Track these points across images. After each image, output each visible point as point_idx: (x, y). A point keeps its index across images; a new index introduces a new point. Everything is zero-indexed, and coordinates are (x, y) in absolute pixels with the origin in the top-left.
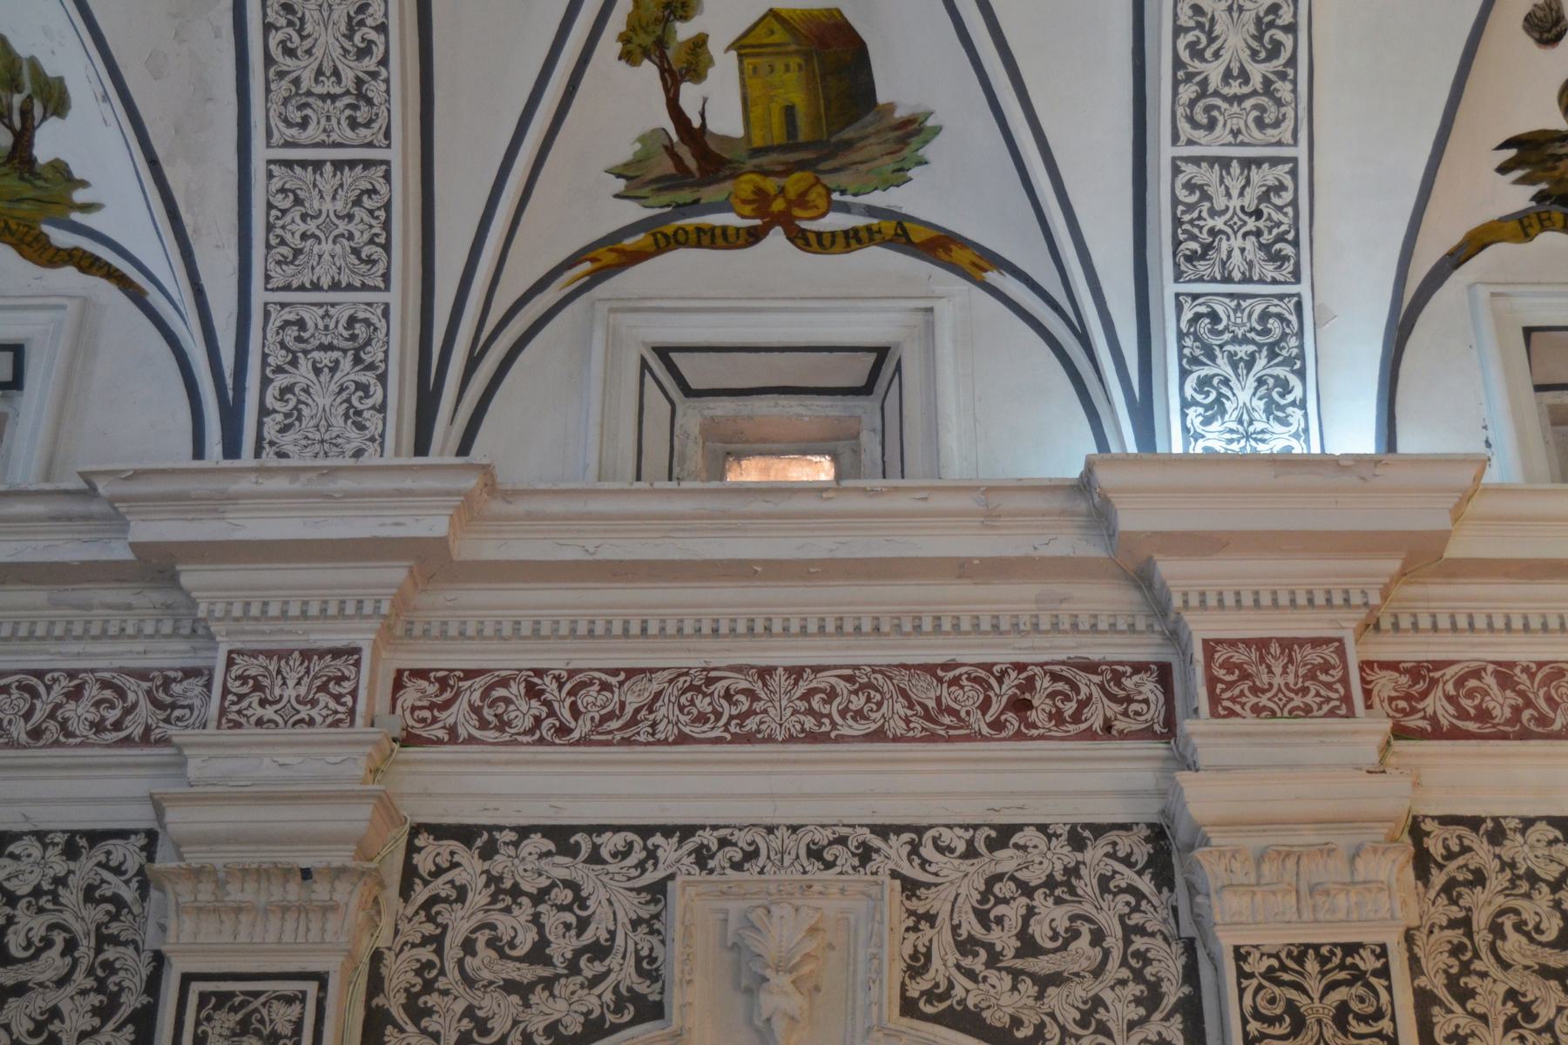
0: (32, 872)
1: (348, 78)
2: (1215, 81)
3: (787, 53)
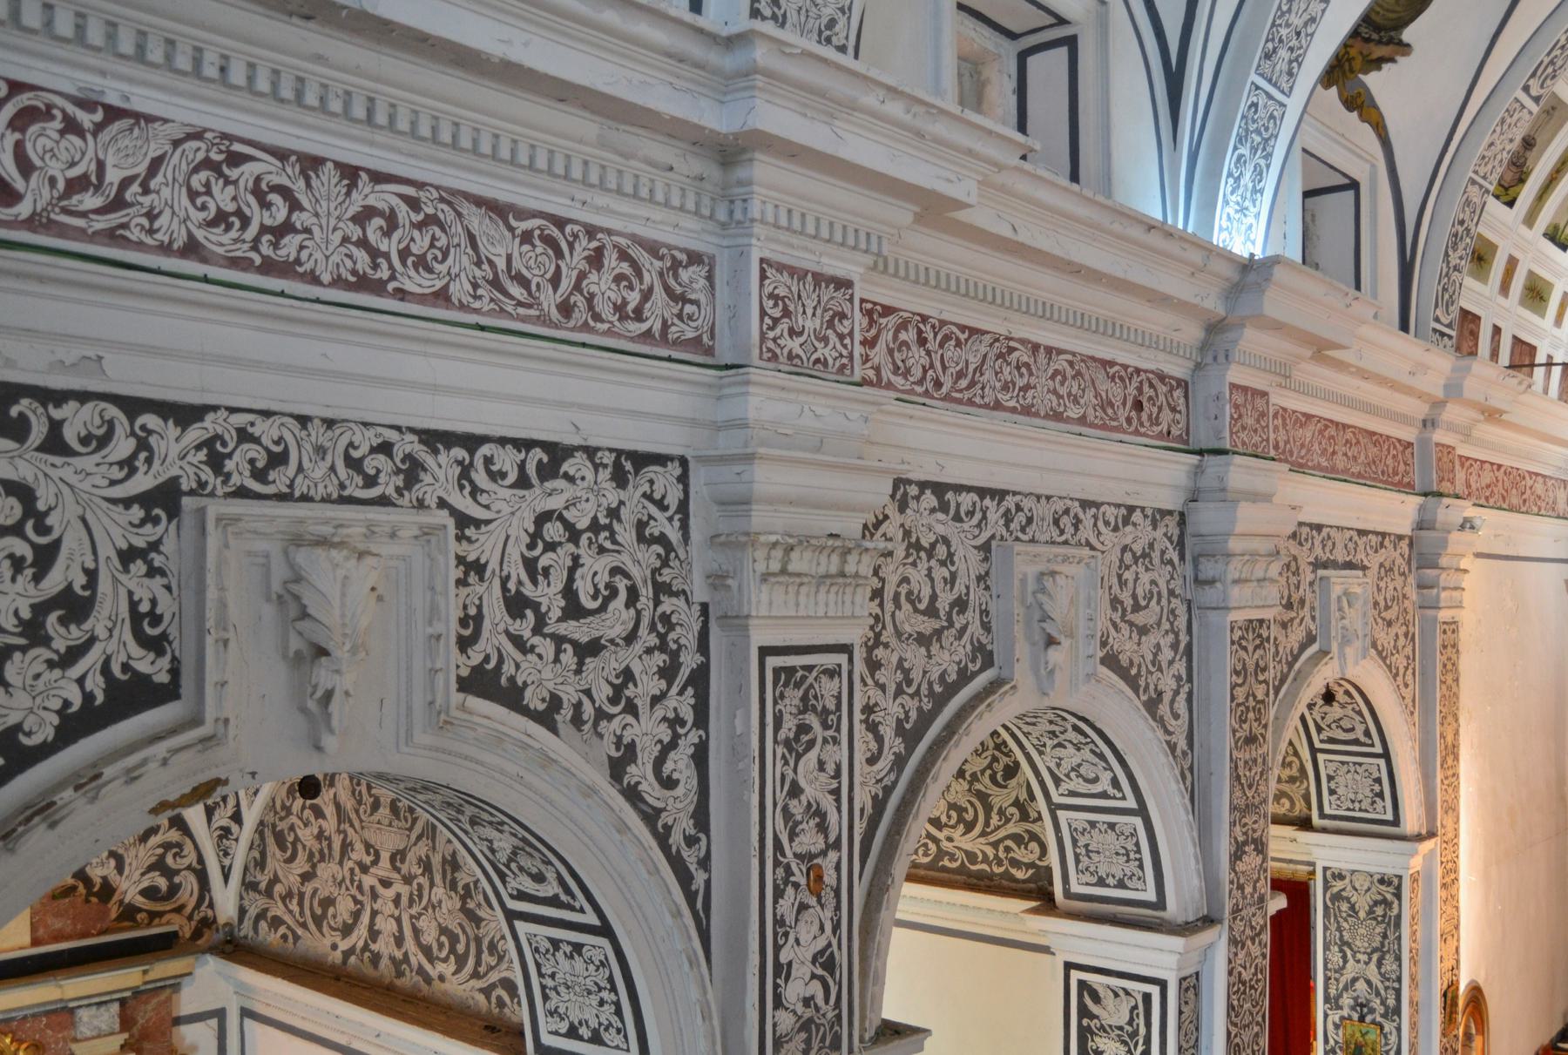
0: (587, 500)
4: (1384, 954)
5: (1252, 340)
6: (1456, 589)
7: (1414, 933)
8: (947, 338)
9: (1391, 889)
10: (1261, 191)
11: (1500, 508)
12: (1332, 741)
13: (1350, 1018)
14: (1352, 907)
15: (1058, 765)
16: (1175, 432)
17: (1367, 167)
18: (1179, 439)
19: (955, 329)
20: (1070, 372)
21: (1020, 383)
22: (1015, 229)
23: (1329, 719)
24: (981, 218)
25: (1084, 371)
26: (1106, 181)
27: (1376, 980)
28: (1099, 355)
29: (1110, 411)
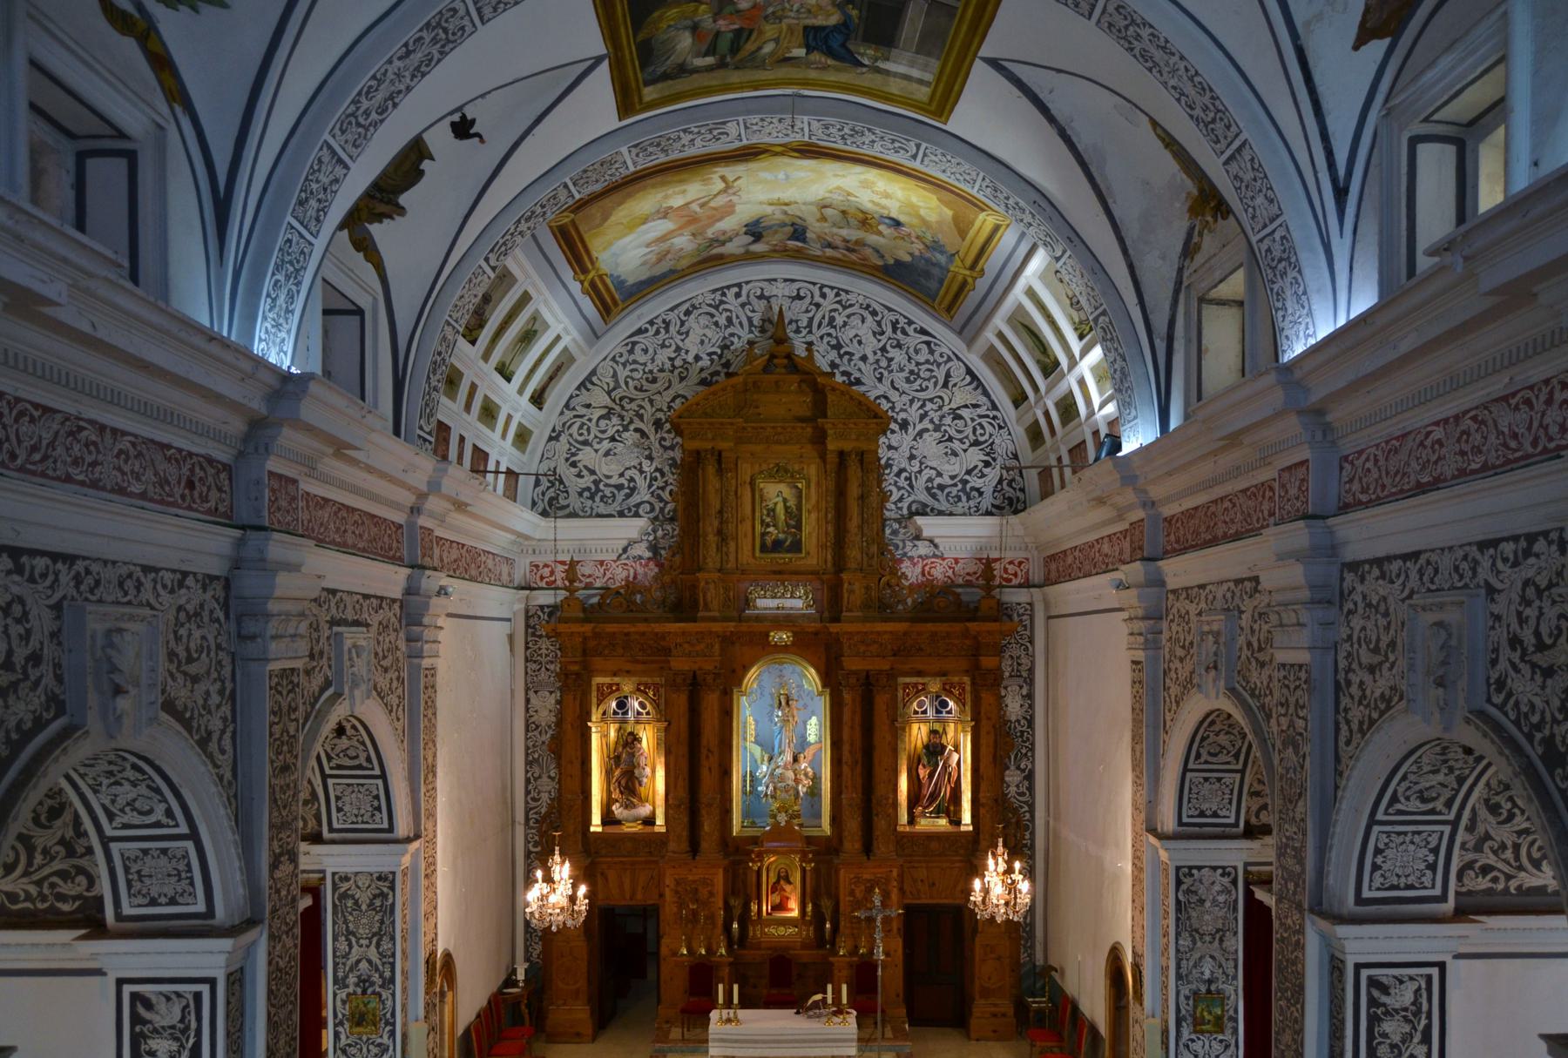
4: (382, 936)
5: (288, 438)
6: (434, 642)
7: (405, 916)
8: (22, 414)
9: (387, 884)
10: (292, 312)
11: (463, 579)
12: (339, 767)
13: (355, 993)
14: (356, 902)
15: (113, 802)
16: (222, 509)
17: (370, 299)
18: (225, 515)
19: (29, 406)
20: (132, 452)
21: (89, 459)
22: (94, 326)
23: (338, 749)
24: (65, 315)
25: (145, 452)
26: (164, 288)
27: (375, 959)
28: (158, 438)
29: (167, 489)
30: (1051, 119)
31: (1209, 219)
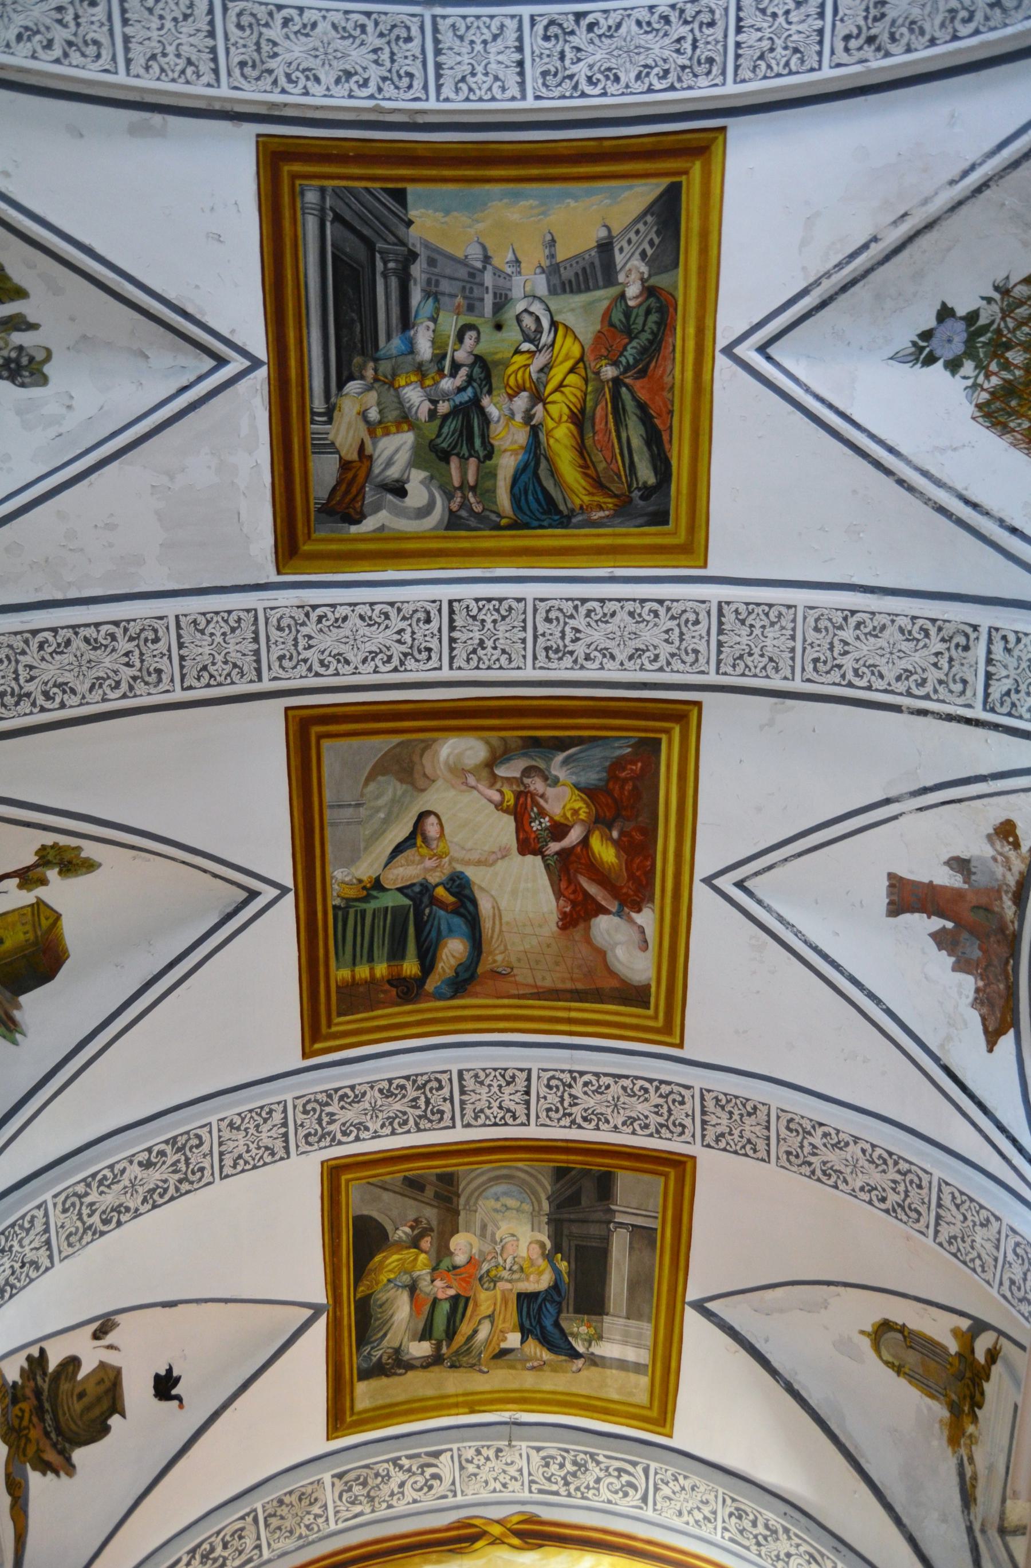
1: (29, 687)
2: (87, 1200)
3: (35, 932)
30: (773, 1372)
31: (971, 1429)
